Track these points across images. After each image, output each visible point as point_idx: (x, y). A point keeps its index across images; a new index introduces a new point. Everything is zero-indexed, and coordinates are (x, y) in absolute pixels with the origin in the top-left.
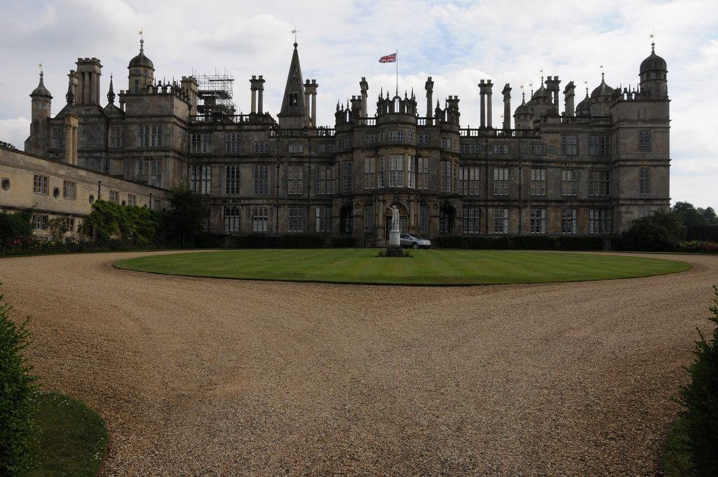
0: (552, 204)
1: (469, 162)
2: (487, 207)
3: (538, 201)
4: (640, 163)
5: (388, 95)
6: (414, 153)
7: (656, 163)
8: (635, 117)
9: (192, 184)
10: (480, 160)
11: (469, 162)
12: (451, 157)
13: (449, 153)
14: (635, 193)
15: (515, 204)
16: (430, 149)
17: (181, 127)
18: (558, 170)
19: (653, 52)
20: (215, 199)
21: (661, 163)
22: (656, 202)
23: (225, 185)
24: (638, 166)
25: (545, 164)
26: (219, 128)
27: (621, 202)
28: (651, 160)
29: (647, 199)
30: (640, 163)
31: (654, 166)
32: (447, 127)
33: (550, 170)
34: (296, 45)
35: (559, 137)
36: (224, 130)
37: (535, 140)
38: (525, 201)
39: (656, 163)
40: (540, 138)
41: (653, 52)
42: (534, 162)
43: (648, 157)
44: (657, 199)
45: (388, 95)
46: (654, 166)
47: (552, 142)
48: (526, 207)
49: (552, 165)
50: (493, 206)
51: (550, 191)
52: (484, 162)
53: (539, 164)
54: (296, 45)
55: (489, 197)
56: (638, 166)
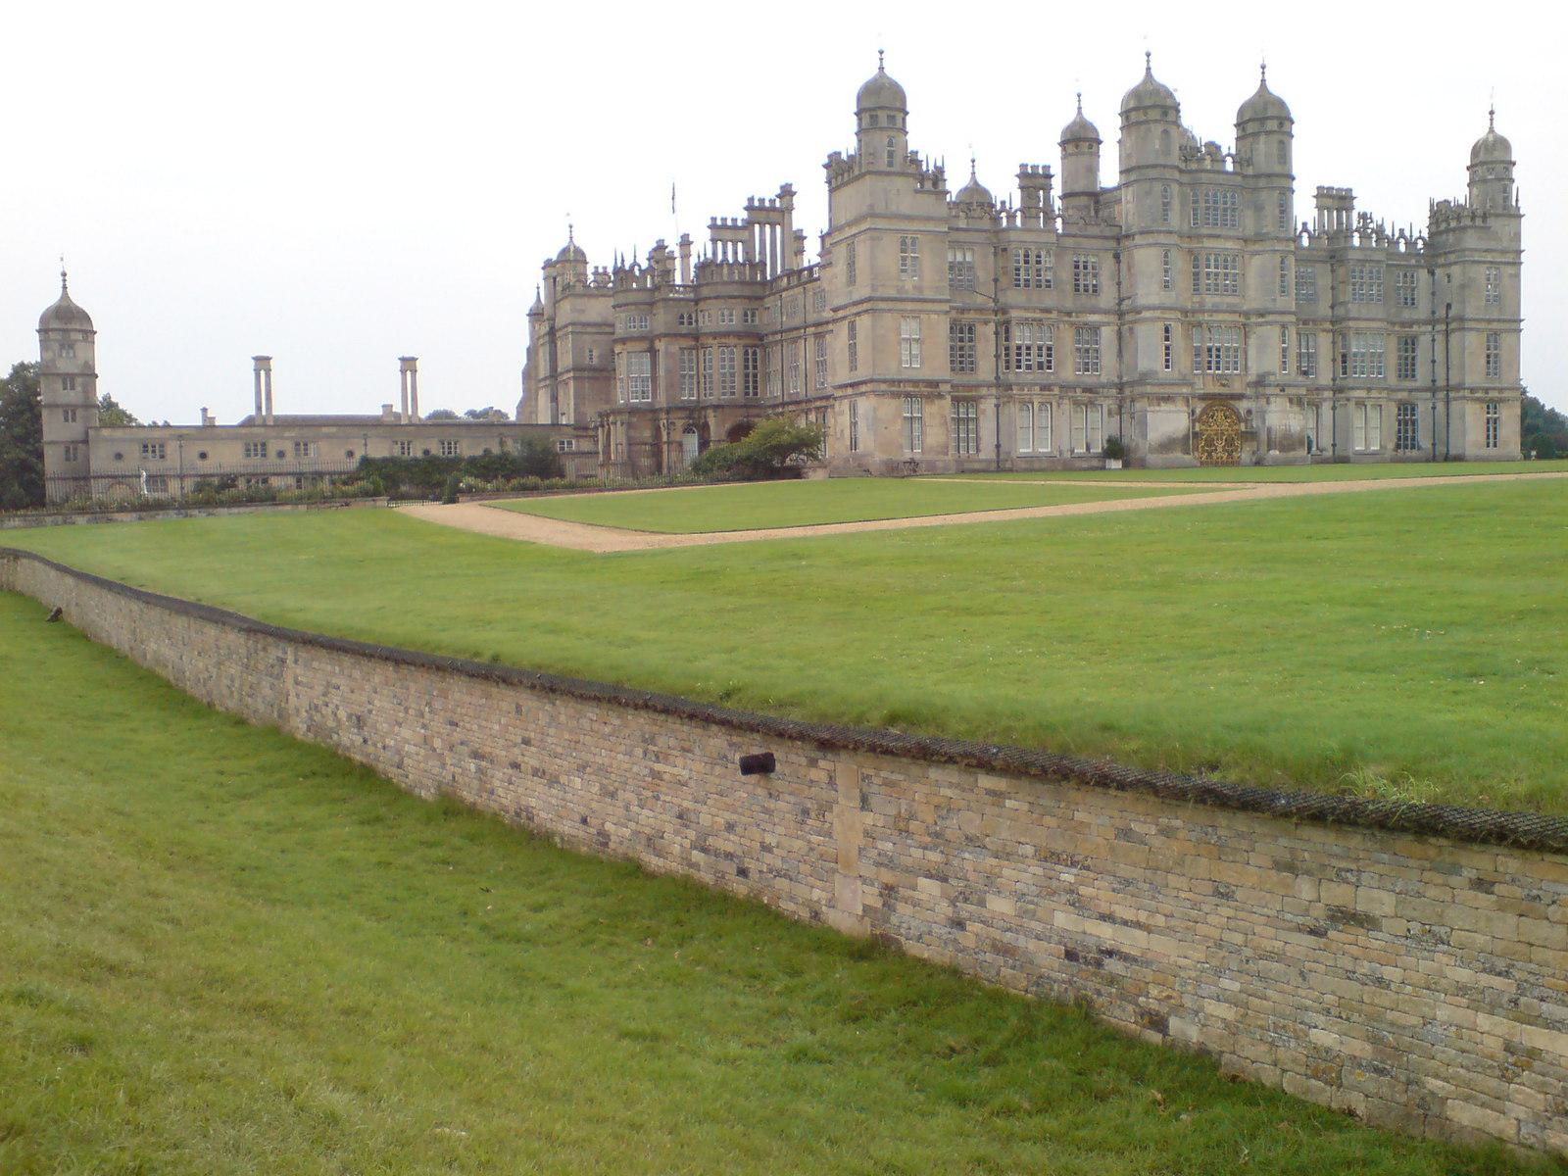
3: (821, 399)
5: (623, 260)
6: (645, 345)
10: (776, 333)
12: (710, 341)
13: (706, 334)
14: (843, 376)
16: (659, 337)
17: (600, 333)
19: (881, 68)
21: (865, 306)
22: (863, 388)
24: (844, 318)
29: (852, 385)
31: (858, 314)
32: (705, 292)
38: (809, 401)
41: (881, 68)
42: (817, 325)
43: (856, 297)
45: (623, 260)
46: (858, 314)
48: (810, 410)
52: (778, 337)
53: (820, 329)
55: (786, 399)
56: (844, 318)
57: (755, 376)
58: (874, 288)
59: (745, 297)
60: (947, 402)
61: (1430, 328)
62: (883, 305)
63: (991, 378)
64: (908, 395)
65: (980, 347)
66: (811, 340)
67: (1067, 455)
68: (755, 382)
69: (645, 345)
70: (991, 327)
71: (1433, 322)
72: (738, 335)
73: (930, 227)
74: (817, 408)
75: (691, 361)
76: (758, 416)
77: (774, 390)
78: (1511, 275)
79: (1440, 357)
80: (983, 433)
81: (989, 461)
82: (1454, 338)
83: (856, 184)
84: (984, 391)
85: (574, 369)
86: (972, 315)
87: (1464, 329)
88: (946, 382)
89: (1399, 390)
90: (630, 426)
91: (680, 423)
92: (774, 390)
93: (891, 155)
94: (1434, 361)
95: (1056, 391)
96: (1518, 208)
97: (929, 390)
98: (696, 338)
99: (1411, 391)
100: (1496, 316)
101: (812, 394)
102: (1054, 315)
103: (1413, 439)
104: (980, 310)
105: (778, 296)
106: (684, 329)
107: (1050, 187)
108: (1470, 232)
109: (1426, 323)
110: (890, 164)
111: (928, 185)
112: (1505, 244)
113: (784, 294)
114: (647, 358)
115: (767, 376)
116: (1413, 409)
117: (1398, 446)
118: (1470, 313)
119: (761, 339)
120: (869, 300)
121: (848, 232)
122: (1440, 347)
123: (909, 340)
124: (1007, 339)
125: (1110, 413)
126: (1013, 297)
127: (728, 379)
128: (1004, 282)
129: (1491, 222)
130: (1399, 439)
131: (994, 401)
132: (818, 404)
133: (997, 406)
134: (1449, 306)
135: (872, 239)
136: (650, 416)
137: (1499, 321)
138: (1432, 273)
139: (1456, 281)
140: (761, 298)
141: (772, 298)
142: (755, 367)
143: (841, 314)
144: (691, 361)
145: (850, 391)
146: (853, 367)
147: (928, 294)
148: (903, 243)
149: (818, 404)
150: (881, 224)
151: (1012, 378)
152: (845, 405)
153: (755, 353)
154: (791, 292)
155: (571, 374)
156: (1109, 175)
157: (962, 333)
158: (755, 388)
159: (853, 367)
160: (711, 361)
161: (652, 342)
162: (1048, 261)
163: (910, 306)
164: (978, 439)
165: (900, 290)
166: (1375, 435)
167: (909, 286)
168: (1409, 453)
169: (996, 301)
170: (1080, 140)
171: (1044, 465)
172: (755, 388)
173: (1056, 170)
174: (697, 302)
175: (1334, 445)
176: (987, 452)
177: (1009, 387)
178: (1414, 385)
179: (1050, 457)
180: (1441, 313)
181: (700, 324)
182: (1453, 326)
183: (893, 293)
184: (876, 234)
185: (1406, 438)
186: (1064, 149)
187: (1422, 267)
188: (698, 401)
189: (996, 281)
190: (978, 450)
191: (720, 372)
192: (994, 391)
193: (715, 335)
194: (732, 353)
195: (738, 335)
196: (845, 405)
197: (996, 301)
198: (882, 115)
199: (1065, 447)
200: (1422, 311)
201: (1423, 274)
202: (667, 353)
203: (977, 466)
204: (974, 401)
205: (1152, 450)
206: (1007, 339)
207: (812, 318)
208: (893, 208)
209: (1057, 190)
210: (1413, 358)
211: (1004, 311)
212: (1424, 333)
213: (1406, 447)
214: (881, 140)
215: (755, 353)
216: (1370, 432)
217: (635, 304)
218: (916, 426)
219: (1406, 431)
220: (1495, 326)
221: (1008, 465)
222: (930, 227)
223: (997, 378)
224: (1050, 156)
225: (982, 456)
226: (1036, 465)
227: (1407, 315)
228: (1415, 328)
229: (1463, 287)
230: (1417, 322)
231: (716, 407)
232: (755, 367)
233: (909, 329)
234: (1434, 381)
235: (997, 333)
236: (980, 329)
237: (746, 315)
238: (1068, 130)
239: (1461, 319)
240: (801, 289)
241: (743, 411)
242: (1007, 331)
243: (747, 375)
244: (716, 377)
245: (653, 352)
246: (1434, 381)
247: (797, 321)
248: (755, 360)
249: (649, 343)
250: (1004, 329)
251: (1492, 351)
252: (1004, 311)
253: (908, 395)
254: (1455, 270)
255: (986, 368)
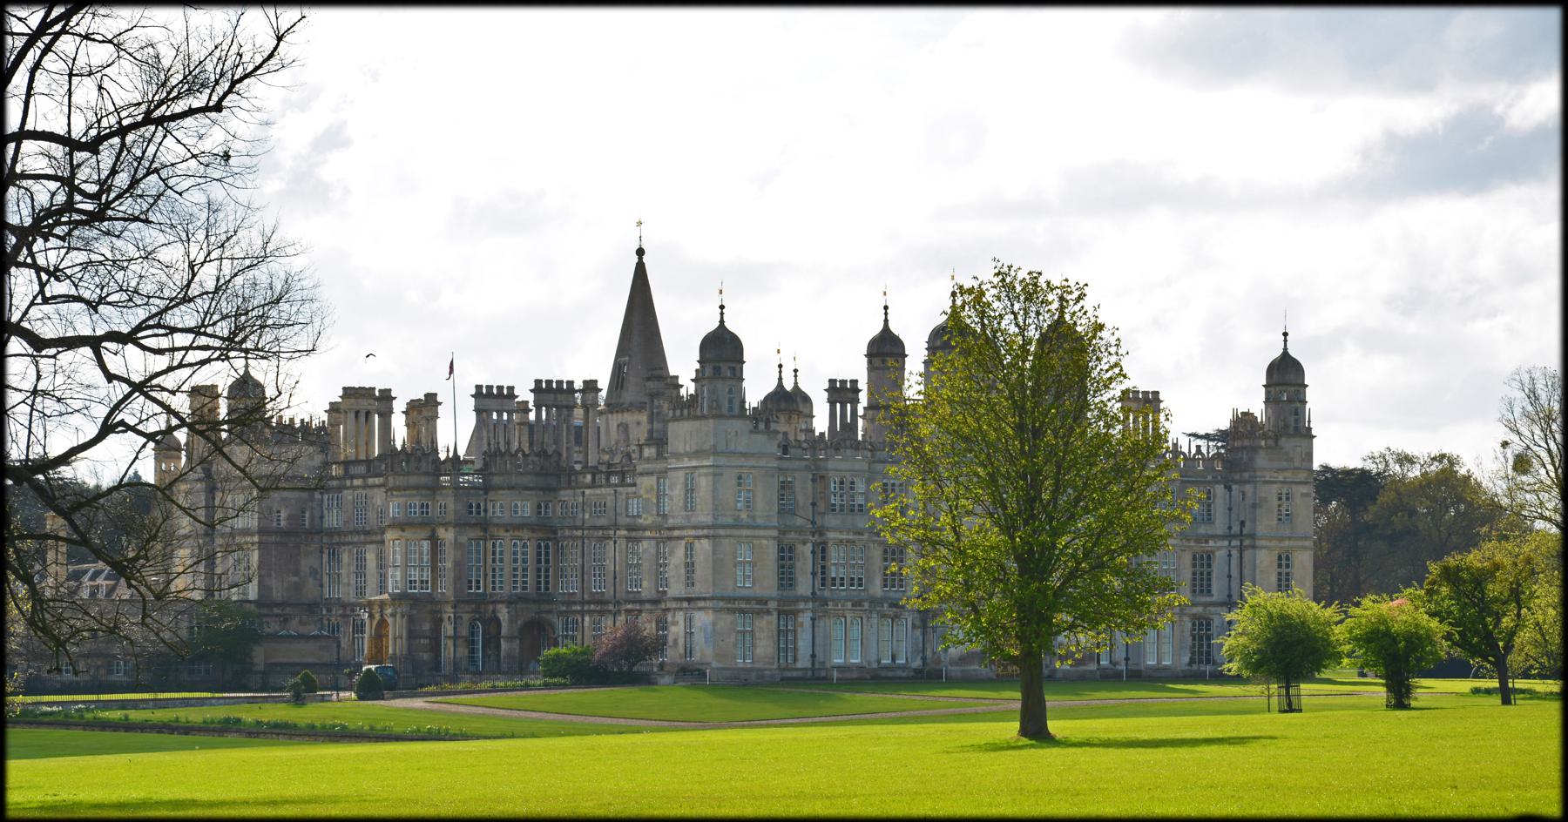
0: (648, 606)
1: (567, 533)
2: (582, 613)
3: (634, 602)
4: (685, 533)
6: (426, 533)
7: (700, 532)
8: (681, 450)
9: (326, 579)
10: (576, 528)
11: (567, 533)
12: (502, 533)
14: (676, 589)
15: (611, 607)
16: (445, 525)
18: (653, 543)
19: (722, 321)
20: (344, 606)
21: (705, 532)
22: (701, 604)
23: (353, 582)
24: (682, 538)
25: (640, 534)
26: (348, 483)
27: (669, 605)
28: (695, 528)
29: (689, 600)
30: (685, 533)
31: (698, 537)
32: (497, 480)
33: (645, 544)
34: (640, 252)
35: (654, 479)
36: (352, 487)
37: (630, 489)
39: (700, 532)
40: (634, 485)
41: (722, 321)
42: (630, 529)
43: (694, 521)
44: (699, 599)
46: (698, 537)
47: (647, 492)
48: (619, 612)
49: (648, 534)
50: (590, 612)
51: (645, 584)
52: (579, 533)
53: (634, 534)
54: (640, 252)
56: (682, 538)
57: (547, 570)
58: (715, 517)
59: (541, 489)
60: (774, 618)
61: (1226, 543)
62: (722, 532)
63: (809, 593)
64: (742, 611)
65: (799, 565)
66: (622, 543)
67: (875, 665)
68: (547, 577)
69: (426, 533)
70: (809, 546)
71: (1229, 537)
72: (532, 528)
73: (763, 463)
74: (627, 611)
75: (478, 552)
76: (550, 612)
77: (569, 587)
78: (1303, 495)
79: (1235, 573)
80: (800, 643)
81: (805, 669)
82: (1247, 554)
83: (697, 424)
84: (801, 606)
85: (262, 531)
86: (792, 535)
87: (1254, 547)
88: (773, 599)
89: (1194, 605)
90: (411, 620)
91: (466, 617)
92: (571, 587)
93: (731, 401)
94: (1229, 576)
95: (866, 605)
96: (1310, 429)
97: (758, 606)
98: (485, 530)
99: (1206, 605)
100: (1288, 533)
101: (621, 595)
102: (866, 536)
103: (1208, 653)
104: (799, 530)
105: (579, 491)
106: (473, 519)
107: (857, 401)
108: (1262, 454)
109: (1223, 537)
110: (731, 409)
111: (762, 426)
112: (1297, 464)
113: (587, 492)
114: (426, 545)
115: (561, 573)
116: (1208, 624)
117: (1192, 661)
118: (1261, 529)
119: (555, 532)
120: (709, 527)
121: (687, 463)
122: (1235, 562)
123: (743, 563)
124: (823, 558)
125: (914, 626)
126: (831, 521)
127: (519, 572)
128: (821, 506)
129: (1283, 442)
130: (1193, 653)
131: (810, 614)
132: (629, 606)
133: (813, 619)
134: (1242, 524)
135: (715, 475)
136: (429, 607)
137: (1290, 538)
138: (1229, 489)
139: (1249, 502)
140: (555, 490)
141: (569, 492)
142: (547, 561)
143: (676, 533)
144: (478, 552)
145: (685, 604)
146: (690, 582)
147: (759, 521)
148: (740, 478)
149: (629, 606)
150: (722, 461)
151: (827, 594)
152: (680, 617)
153: (547, 547)
154: (598, 491)
155: (256, 539)
156: (913, 388)
157: (786, 555)
158: (547, 583)
159: (690, 582)
160: (501, 553)
161: (434, 532)
162: (860, 487)
163: (744, 532)
164: (795, 650)
165: (737, 518)
166: (1167, 649)
167: (744, 516)
168: (1203, 668)
169: (813, 523)
170: (885, 349)
171: (855, 675)
172: (547, 583)
173: (863, 385)
174: (486, 488)
175: (1127, 659)
176: (804, 662)
177: (825, 602)
178: (1208, 599)
179: (860, 668)
180: (1236, 529)
181: (490, 514)
182: (1247, 542)
183: (730, 520)
184: (718, 471)
185: (1201, 653)
186: (870, 362)
187: (1217, 482)
188: (484, 594)
189: (814, 504)
190: (795, 660)
191: (509, 564)
192: (810, 605)
193: (508, 527)
194: (524, 546)
195: (532, 528)
196: (680, 617)
197: (813, 523)
198: (725, 367)
199: (873, 658)
200: (1219, 526)
201: (1220, 489)
202: (457, 545)
203: (795, 674)
204: (796, 613)
205: (952, 663)
206: (823, 558)
207: (623, 520)
208: (732, 448)
209: (863, 398)
210: (1209, 574)
211: (821, 531)
212: (1220, 548)
213: (1200, 662)
214: (722, 387)
215: (547, 547)
216: (1162, 646)
217: (416, 488)
218: (748, 638)
219: (1201, 646)
220: (1287, 543)
221: (823, 674)
222: (763, 463)
223: (813, 593)
224: (856, 369)
225: (799, 665)
226: (848, 675)
227: (1202, 530)
228: (1211, 543)
229: (1254, 506)
230: (1214, 537)
231: (510, 602)
232: (547, 561)
233: (745, 554)
234: (1230, 596)
235: (813, 552)
236: (800, 548)
237: (539, 507)
238: (874, 344)
239: (1252, 536)
240: (610, 490)
241: (534, 607)
242: (823, 550)
243: (539, 570)
244: (507, 570)
245: (434, 540)
246: (1230, 596)
247: (602, 522)
248: (547, 554)
249: (428, 526)
250: (821, 551)
251: (1284, 570)
252: (821, 531)
253: (742, 611)
254: (1249, 488)
255: (804, 586)
